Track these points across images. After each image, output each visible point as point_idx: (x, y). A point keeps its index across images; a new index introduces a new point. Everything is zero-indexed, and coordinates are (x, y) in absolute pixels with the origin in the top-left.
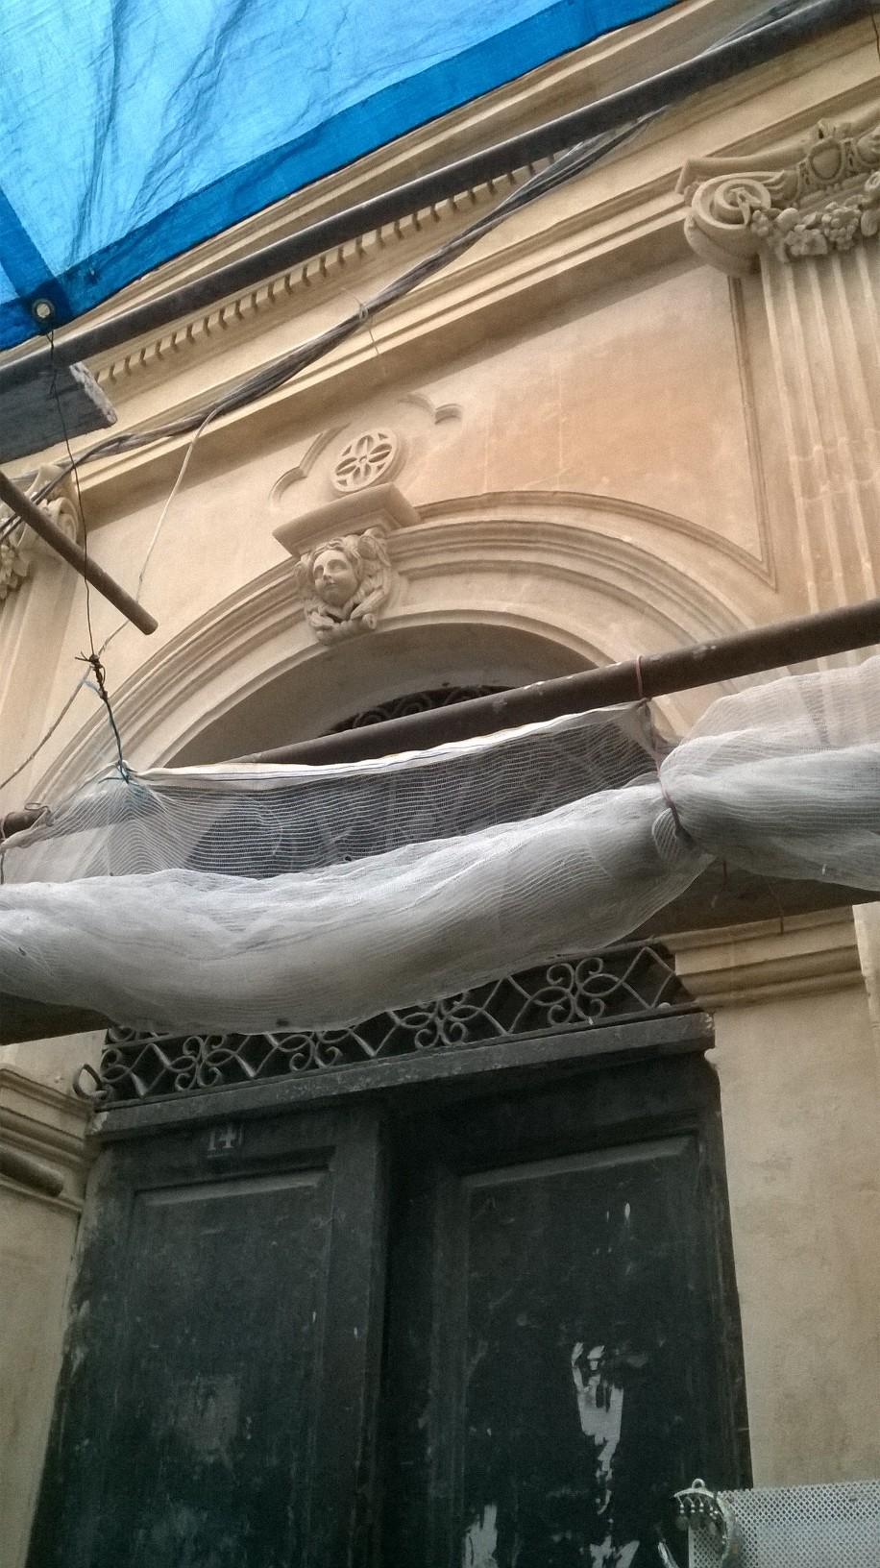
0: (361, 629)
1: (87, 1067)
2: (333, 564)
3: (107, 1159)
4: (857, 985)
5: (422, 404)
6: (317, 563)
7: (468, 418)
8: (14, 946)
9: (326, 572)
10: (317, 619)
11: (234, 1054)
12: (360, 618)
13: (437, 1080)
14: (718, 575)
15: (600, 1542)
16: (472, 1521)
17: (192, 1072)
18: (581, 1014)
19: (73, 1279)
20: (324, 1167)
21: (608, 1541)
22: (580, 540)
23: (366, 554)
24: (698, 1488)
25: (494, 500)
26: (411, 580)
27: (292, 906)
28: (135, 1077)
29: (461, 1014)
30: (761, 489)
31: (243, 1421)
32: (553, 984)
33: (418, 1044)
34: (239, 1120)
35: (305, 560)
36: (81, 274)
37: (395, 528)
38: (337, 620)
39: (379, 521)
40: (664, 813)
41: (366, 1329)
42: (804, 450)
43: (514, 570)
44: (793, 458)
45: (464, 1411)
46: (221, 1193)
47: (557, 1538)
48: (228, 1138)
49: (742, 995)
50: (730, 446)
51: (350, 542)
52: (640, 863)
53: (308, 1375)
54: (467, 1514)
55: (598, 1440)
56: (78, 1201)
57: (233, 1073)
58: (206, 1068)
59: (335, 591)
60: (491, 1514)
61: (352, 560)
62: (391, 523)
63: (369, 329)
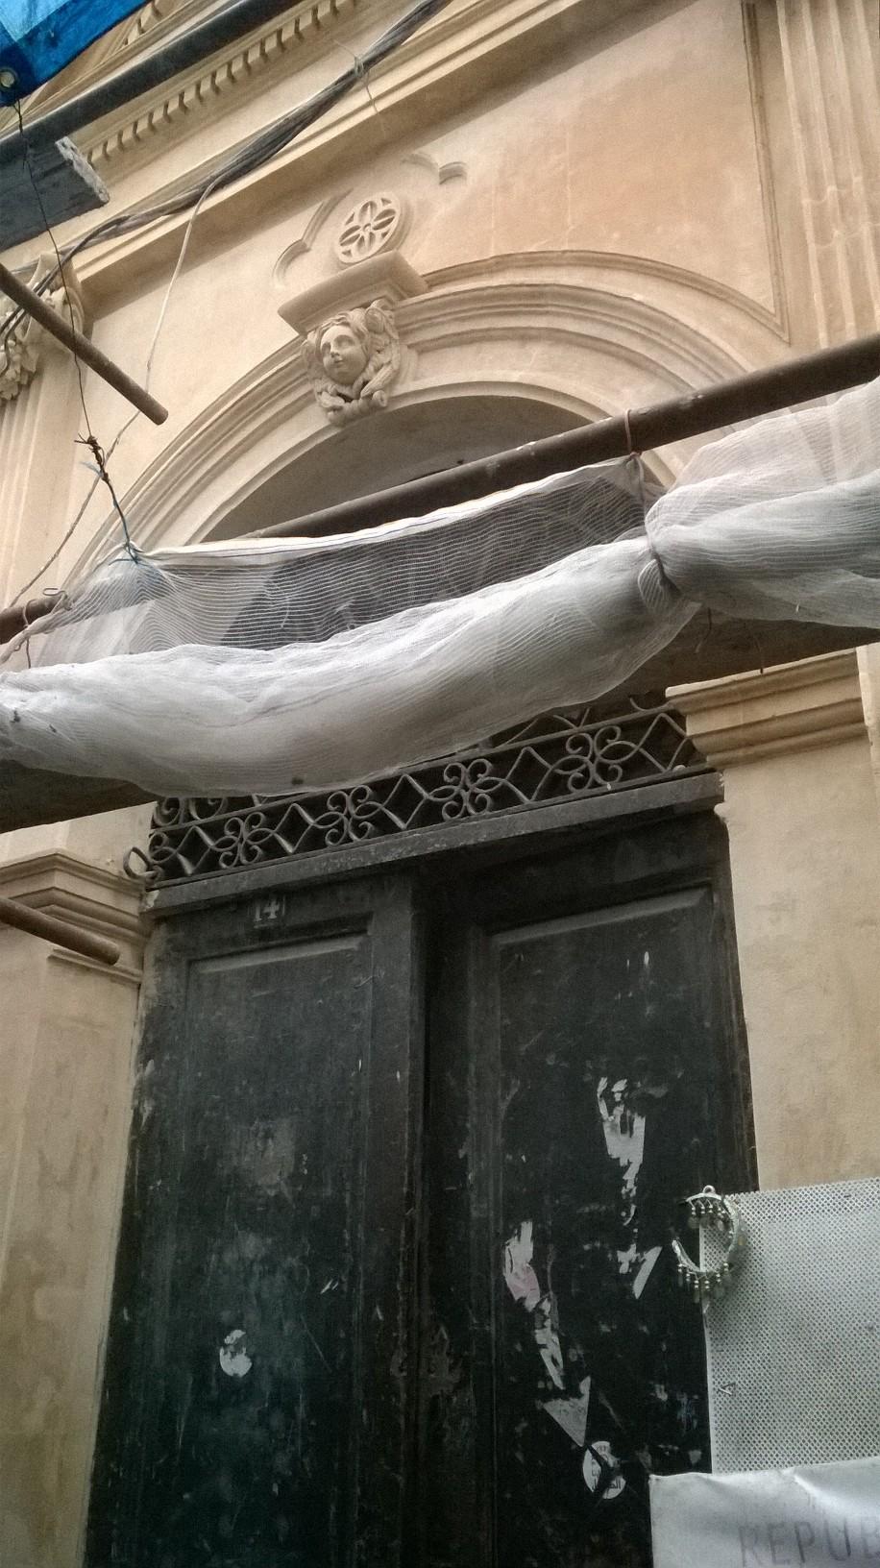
0: (373, 408)
1: (135, 850)
2: (340, 340)
3: (161, 934)
4: (861, 736)
5: (428, 165)
7: (473, 174)
8: (44, 725)
9: (333, 350)
10: (327, 400)
11: (272, 833)
12: (370, 396)
13: (465, 848)
14: (730, 331)
15: (625, 1249)
16: (508, 1235)
17: (235, 851)
18: (600, 780)
19: (138, 1039)
20: (362, 932)
21: (633, 1247)
22: (587, 301)
23: (373, 328)
24: (708, 1193)
25: (502, 263)
27: (304, 672)
28: (181, 858)
29: (485, 786)
30: (774, 239)
31: (299, 1159)
32: (573, 754)
33: (446, 816)
34: (281, 893)
35: (312, 338)
36: (41, 37)
37: (402, 298)
38: (347, 399)
39: (385, 292)
40: (650, 564)
41: (407, 1073)
42: (817, 192)
43: (524, 337)
44: (806, 201)
45: (500, 1140)
46: (271, 958)
47: (587, 1247)
48: (272, 910)
49: (751, 751)
50: (742, 192)
51: (356, 316)
52: (628, 614)
53: (357, 1115)
54: (506, 1226)
55: (623, 1162)
56: (137, 971)
57: (273, 850)
58: (247, 846)
59: (344, 368)
60: (527, 1229)
61: (360, 335)
62: (396, 292)
63: (366, 86)
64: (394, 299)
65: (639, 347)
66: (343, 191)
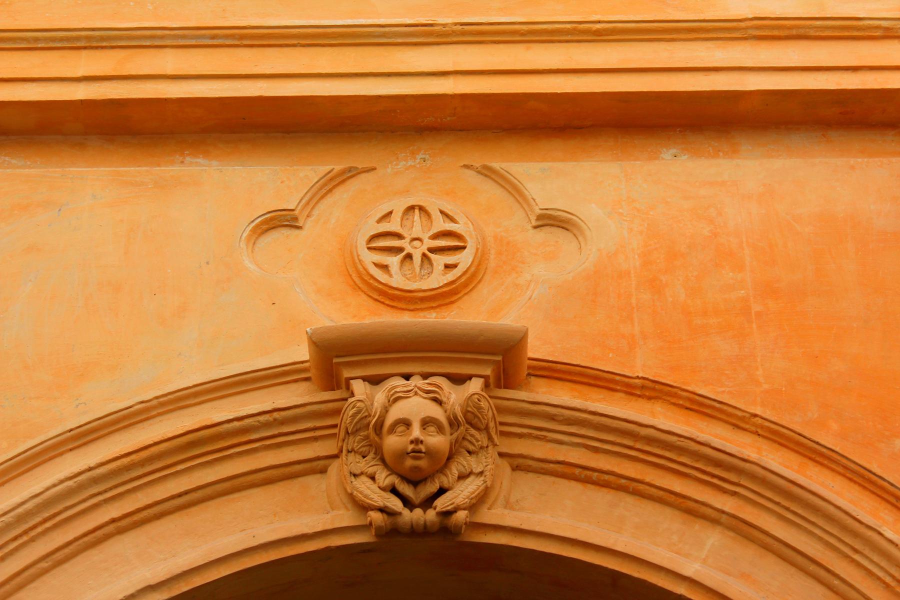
0: (445, 529)
2: (426, 423)
6: (396, 412)
9: (416, 432)
10: (372, 492)
26: (516, 468)
37: (499, 386)
38: (407, 502)
39: (488, 371)
51: (455, 396)
59: (423, 463)
61: (454, 423)
62: (498, 379)
64: (491, 381)
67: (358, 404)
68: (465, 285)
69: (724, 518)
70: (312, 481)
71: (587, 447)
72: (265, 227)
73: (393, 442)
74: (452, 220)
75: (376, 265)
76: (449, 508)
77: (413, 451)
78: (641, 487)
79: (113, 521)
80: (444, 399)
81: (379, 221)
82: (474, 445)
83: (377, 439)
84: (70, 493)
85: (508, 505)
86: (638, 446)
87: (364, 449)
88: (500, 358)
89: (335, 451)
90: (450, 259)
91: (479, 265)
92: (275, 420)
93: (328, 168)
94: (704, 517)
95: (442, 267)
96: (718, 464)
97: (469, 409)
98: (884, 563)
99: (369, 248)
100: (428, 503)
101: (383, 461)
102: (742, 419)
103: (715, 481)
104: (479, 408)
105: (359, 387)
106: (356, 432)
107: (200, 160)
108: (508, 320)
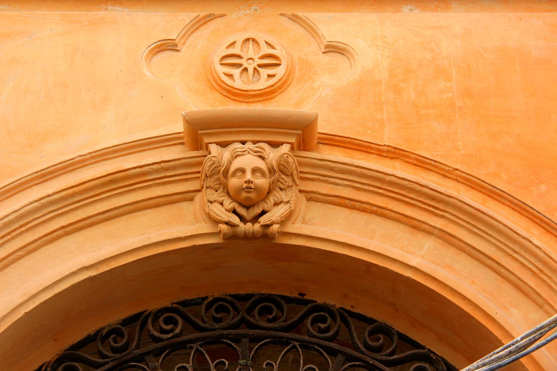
0: (265, 236)
2: (255, 171)
6: (236, 164)
9: (249, 176)
12: (267, 226)
26: (309, 200)
38: (242, 218)
39: (293, 140)
51: (273, 155)
59: (252, 195)
64: (295, 146)
65: (531, 282)
66: (216, 11)
67: (214, 159)
68: (280, 88)
69: (436, 231)
70: (184, 205)
71: (353, 187)
72: (157, 50)
73: (234, 182)
74: (273, 47)
75: (225, 74)
76: (268, 223)
77: (247, 188)
78: (386, 212)
79: (63, 227)
80: (266, 157)
81: (228, 47)
82: (284, 185)
83: (224, 180)
84: (37, 210)
85: (304, 222)
86: (384, 187)
87: (216, 186)
88: (300, 132)
89: (199, 188)
90: (271, 71)
91: (289, 75)
92: (162, 168)
93: (196, 14)
94: (424, 231)
95: (266, 76)
96: (433, 198)
97: (281, 163)
98: (532, 260)
99: (221, 64)
100: (255, 219)
101: (228, 193)
102: (448, 171)
103: (431, 209)
104: (288, 162)
105: (214, 149)
106: (212, 176)
107: (118, 8)
108: (307, 109)
